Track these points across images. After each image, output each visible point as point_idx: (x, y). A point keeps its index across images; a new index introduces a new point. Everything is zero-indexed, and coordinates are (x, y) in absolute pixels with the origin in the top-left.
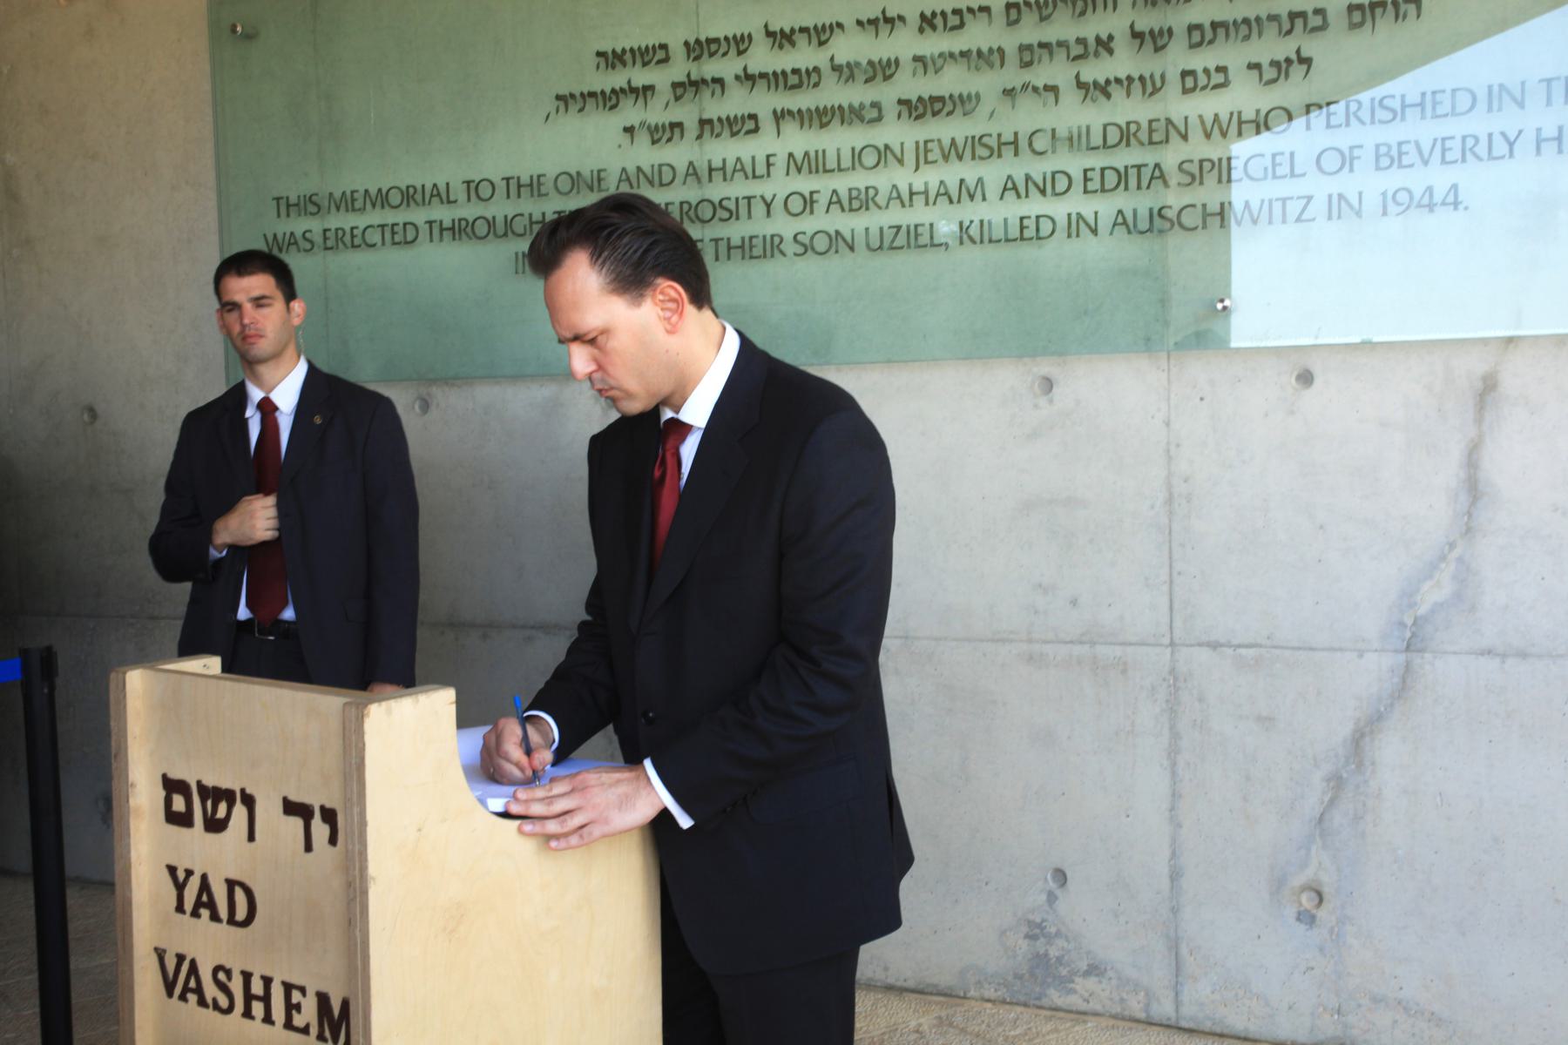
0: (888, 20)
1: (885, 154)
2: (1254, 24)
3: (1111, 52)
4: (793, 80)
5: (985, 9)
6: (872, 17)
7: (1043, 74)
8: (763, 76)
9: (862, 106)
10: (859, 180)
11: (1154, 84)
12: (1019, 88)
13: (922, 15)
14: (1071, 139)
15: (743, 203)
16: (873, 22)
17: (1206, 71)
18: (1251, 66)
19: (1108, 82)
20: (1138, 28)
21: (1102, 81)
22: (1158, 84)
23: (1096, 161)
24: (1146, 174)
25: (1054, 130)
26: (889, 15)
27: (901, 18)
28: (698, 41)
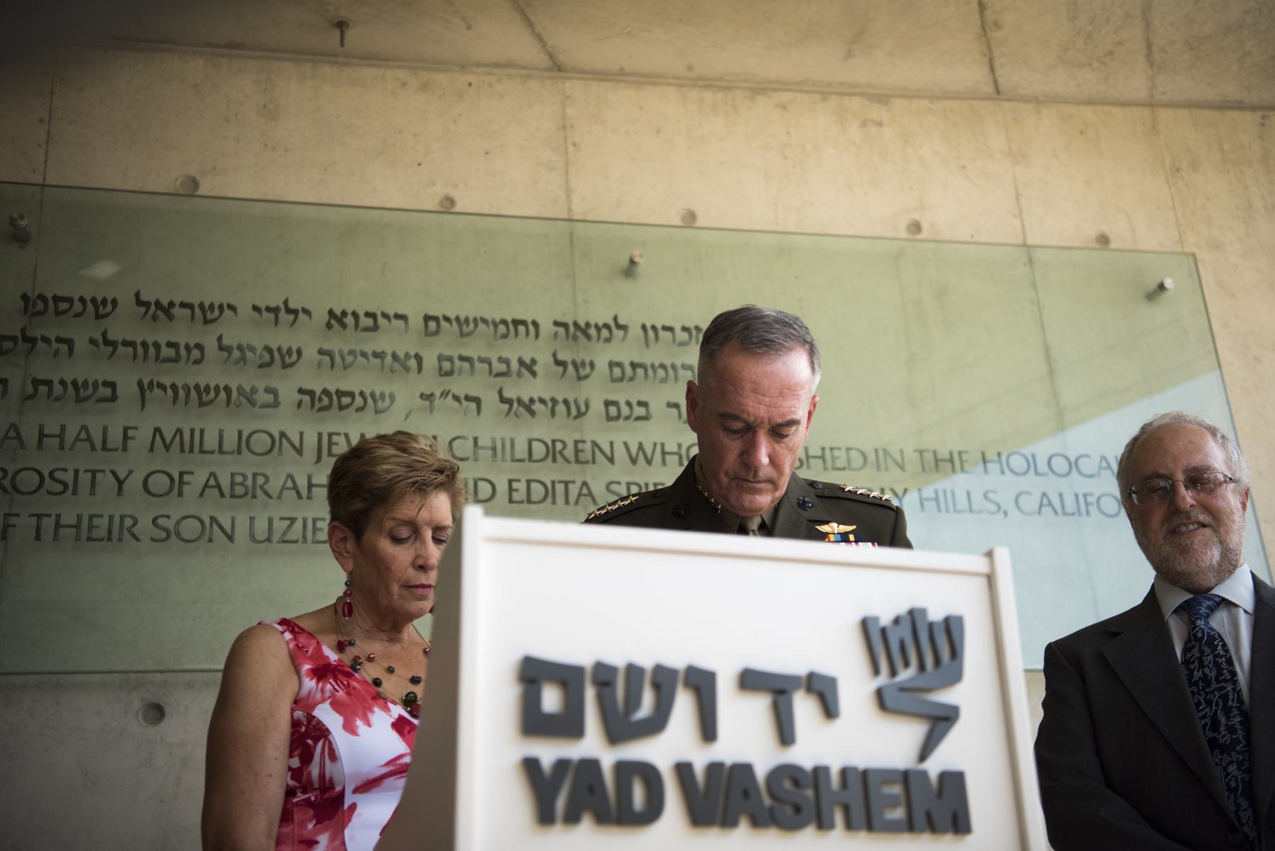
0: (289, 311)
1: (278, 442)
2: (671, 371)
3: (534, 374)
4: (166, 352)
5: (403, 318)
6: (273, 305)
7: (461, 386)
8: (126, 343)
9: (254, 390)
10: (247, 465)
11: (578, 408)
12: (438, 394)
13: (331, 312)
14: (494, 449)
15: (85, 478)
16: (274, 310)
17: (629, 404)
18: (670, 405)
19: (532, 401)
20: (560, 357)
21: (526, 399)
22: (583, 409)
23: (522, 473)
24: (574, 490)
25: (476, 439)
26: (292, 305)
27: (306, 312)
28: (41, 297)
